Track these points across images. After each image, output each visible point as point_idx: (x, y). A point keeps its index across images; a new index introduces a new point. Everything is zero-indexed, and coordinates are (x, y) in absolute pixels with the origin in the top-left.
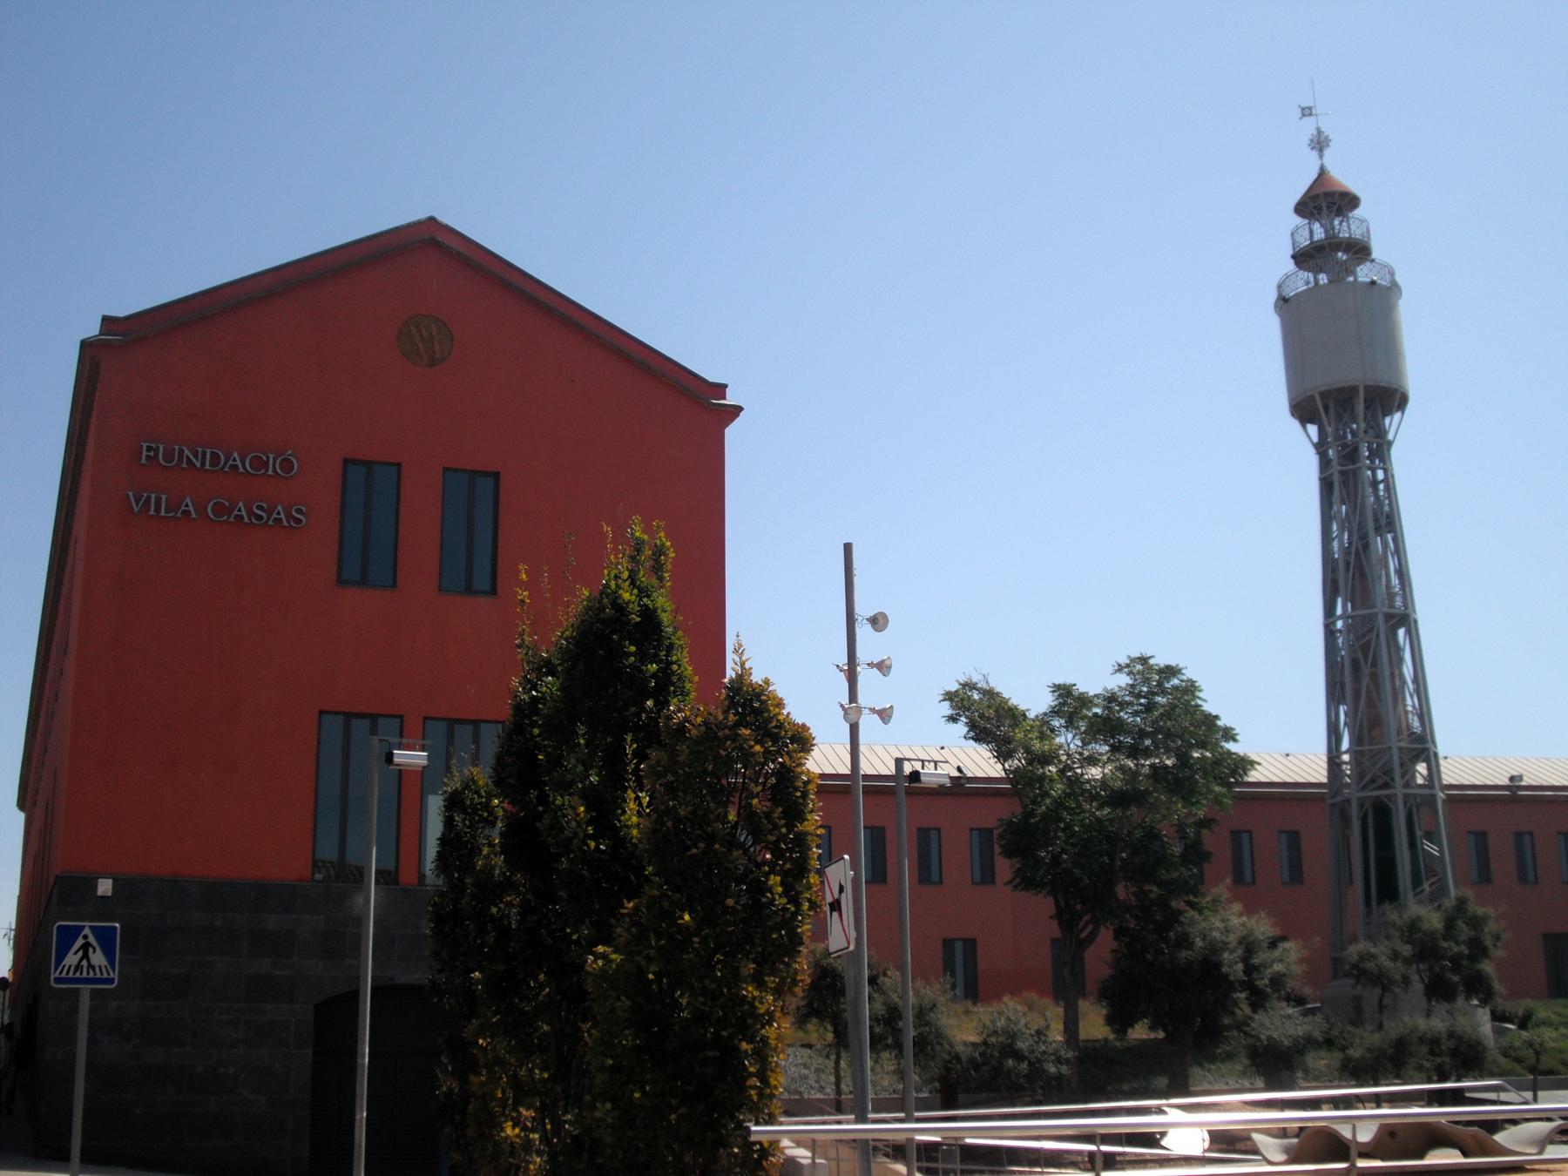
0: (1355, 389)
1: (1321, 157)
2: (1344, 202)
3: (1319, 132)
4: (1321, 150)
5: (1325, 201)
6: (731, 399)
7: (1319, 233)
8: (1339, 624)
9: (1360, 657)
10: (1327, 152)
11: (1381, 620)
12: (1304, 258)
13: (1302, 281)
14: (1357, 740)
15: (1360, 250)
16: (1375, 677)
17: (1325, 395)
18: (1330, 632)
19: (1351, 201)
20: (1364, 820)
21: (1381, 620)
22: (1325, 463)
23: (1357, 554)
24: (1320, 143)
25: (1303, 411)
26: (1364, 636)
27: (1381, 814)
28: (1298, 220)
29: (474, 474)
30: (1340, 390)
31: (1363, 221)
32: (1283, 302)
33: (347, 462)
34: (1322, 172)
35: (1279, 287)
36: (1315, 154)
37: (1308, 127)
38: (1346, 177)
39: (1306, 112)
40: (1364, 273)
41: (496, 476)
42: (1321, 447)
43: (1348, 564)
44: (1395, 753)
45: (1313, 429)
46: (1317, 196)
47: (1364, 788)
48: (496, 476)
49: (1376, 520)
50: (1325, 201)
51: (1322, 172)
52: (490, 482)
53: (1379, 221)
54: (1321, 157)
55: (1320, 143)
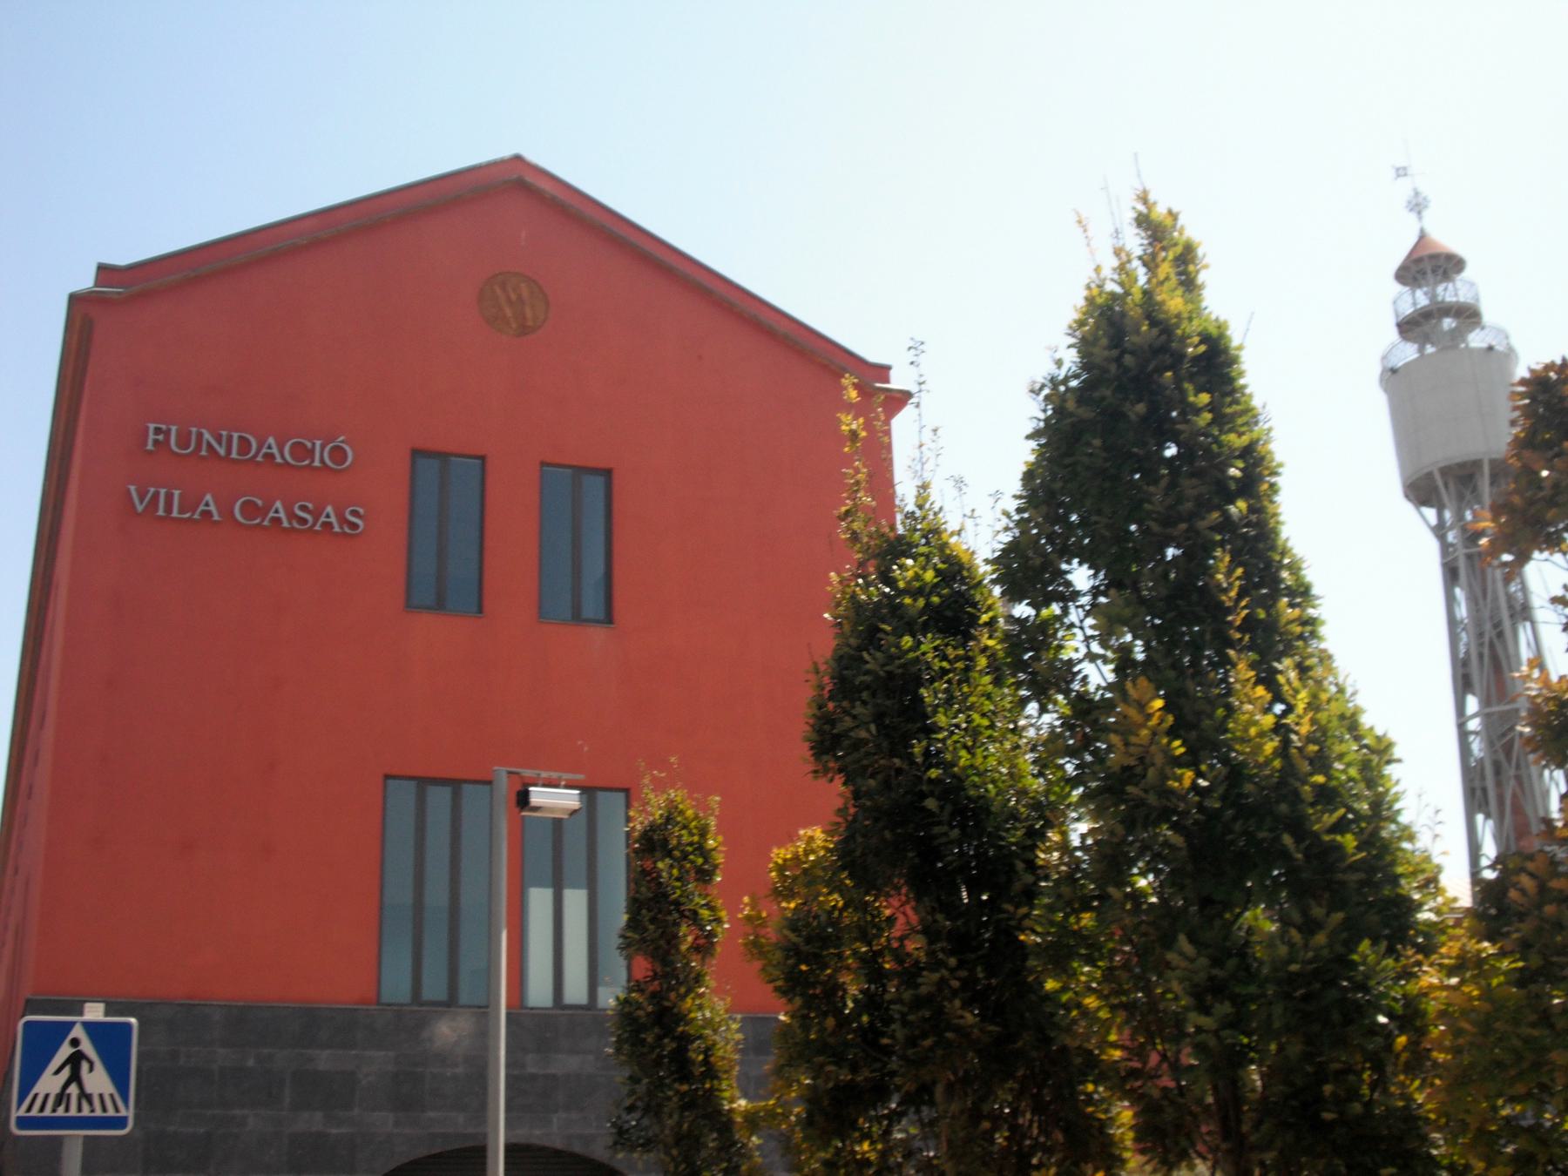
0: (1477, 464)
1: (1420, 218)
3: (1417, 194)
4: (1419, 213)
5: (1427, 265)
6: (897, 382)
7: (1422, 300)
8: (1474, 725)
9: (1502, 757)
10: (1425, 213)
12: (1409, 327)
13: (1408, 352)
17: (1445, 471)
18: (1463, 735)
22: (1445, 547)
23: (1492, 645)
24: (1417, 206)
25: (1421, 491)
26: (1504, 735)
28: (1398, 288)
29: (581, 470)
30: (1462, 465)
31: (1472, 284)
33: (417, 453)
34: (1423, 236)
35: (1384, 358)
36: (1413, 216)
37: (1404, 189)
38: (1447, 239)
39: (1401, 172)
40: (1476, 340)
41: (608, 473)
42: (1439, 531)
43: (1481, 656)
45: (1431, 514)
46: (1419, 260)
48: (608, 473)
49: (1511, 607)
50: (1427, 265)
51: (1423, 236)
52: (599, 481)
54: (1420, 218)
55: (1417, 206)
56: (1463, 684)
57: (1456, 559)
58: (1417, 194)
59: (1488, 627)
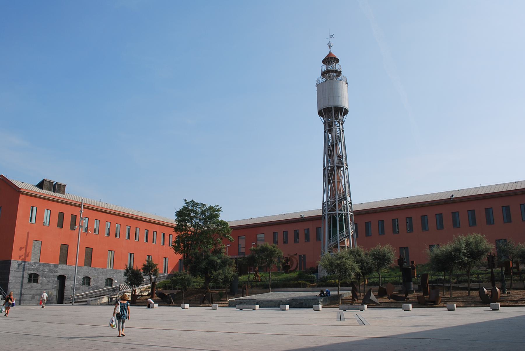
0: (331, 107)
3: (330, 42)
5: (330, 59)
11: (336, 167)
12: (324, 74)
15: (339, 73)
16: (334, 182)
19: (337, 61)
21: (336, 167)
25: (320, 113)
27: (332, 219)
32: (317, 85)
34: (330, 53)
38: (336, 54)
44: (337, 202)
47: (329, 211)
50: (330, 59)
51: (330, 53)
58: (330, 42)
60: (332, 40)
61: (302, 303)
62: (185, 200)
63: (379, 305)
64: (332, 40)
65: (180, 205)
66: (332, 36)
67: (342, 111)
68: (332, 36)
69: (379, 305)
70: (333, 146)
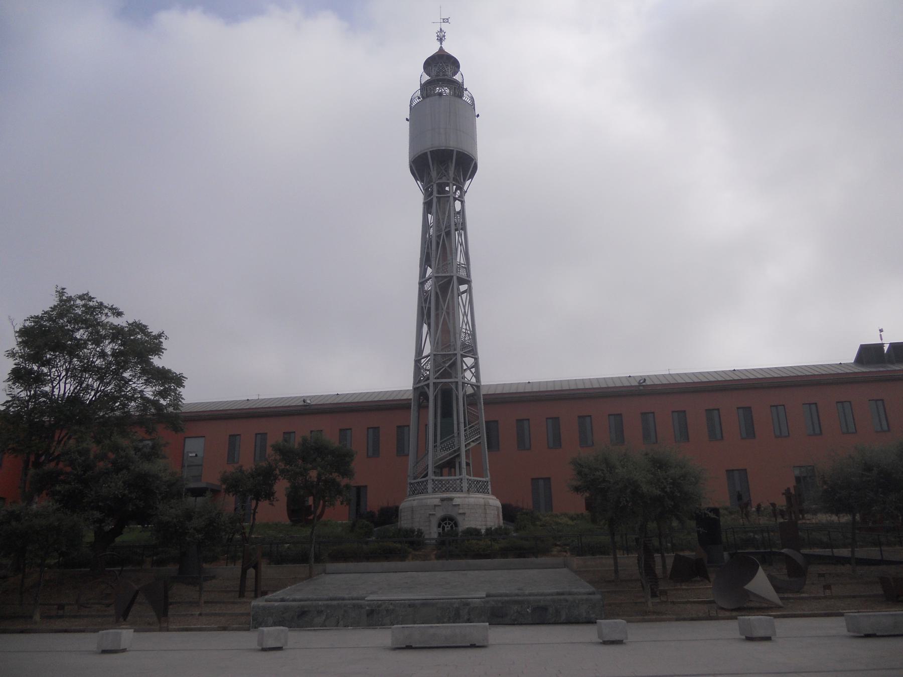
0: (452, 151)
2: (454, 63)
11: (455, 279)
14: (435, 344)
20: (436, 397)
24: (441, 39)
34: (441, 49)
47: (437, 378)
51: (441, 49)
53: (469, 75)
55: (441, 39)
56: (426, 260)
57: (432, 199)
59: (443, 233)
60: (445, 27)
61: (544, 609)
62: (61, 293)
63: (779, 608)
64: (445, 27)
65: (43, 302)
66: (446, 20)
67: (465, 165)
68: (446, 20)
69: (779, 608)
70: (448, 234)
